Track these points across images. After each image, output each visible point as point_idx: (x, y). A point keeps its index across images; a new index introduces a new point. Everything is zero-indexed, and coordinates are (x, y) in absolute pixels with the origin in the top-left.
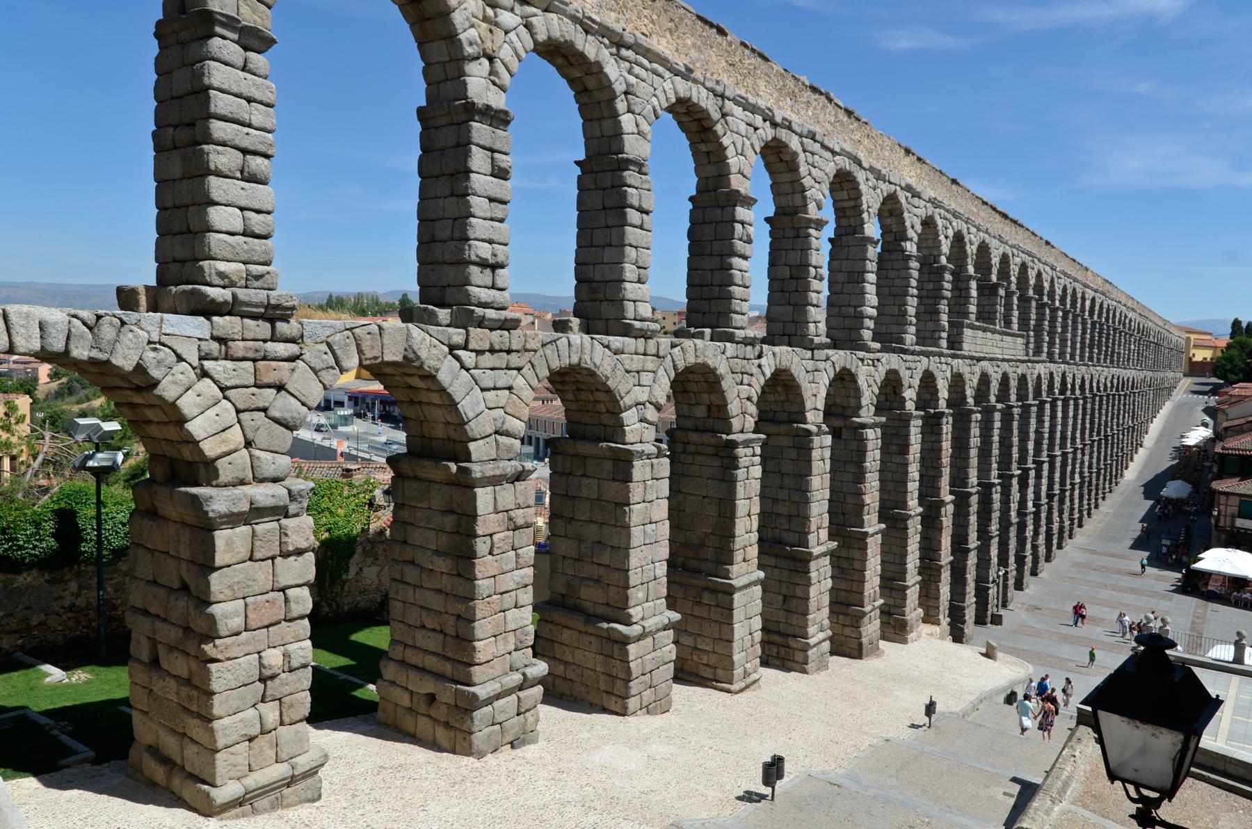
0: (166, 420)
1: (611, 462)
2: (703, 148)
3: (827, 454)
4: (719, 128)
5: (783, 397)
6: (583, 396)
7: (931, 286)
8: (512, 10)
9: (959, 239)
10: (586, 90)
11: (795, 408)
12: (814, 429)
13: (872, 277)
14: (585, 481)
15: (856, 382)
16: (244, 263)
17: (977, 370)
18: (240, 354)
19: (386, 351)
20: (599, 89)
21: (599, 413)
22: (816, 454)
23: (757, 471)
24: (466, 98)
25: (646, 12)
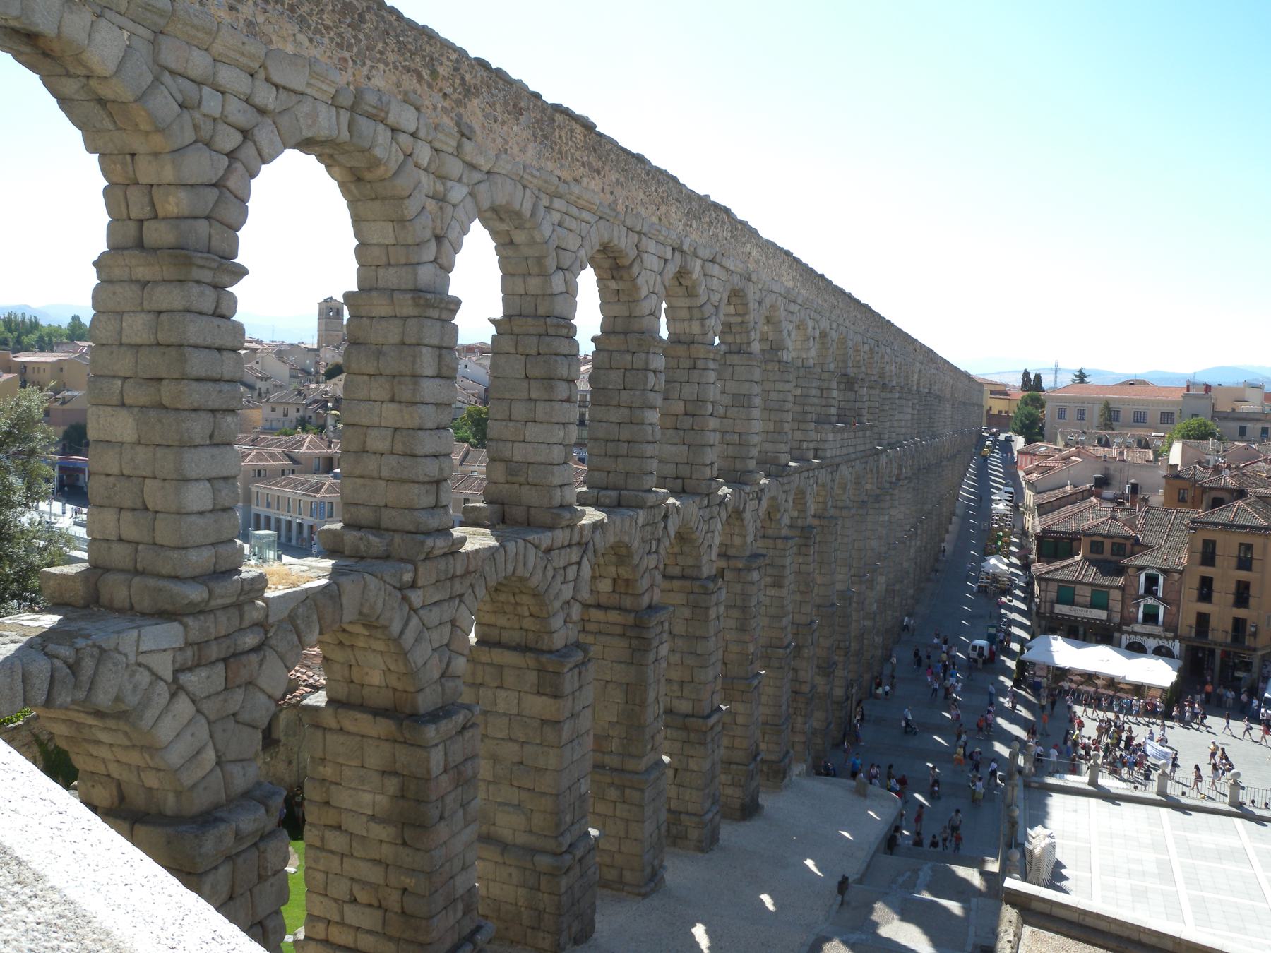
0: (128, 743)
1: (535, 673)
2: (613, 285)
3: (722, 609)
4: (636, 269)
5: (677, 549)
6: (502, 597)
7: (798, 392)
8: (460, 180)
9: (824, 335)
10: (512, 243)
11: (690, 562)
13: (757, 401)
14: (501, 694)
15: (742, 520)
18: (214, 658)
19: (345, 612)
21: (521, 617)
22: (712, 613)
23: (664, 650)
25: (578, 154)
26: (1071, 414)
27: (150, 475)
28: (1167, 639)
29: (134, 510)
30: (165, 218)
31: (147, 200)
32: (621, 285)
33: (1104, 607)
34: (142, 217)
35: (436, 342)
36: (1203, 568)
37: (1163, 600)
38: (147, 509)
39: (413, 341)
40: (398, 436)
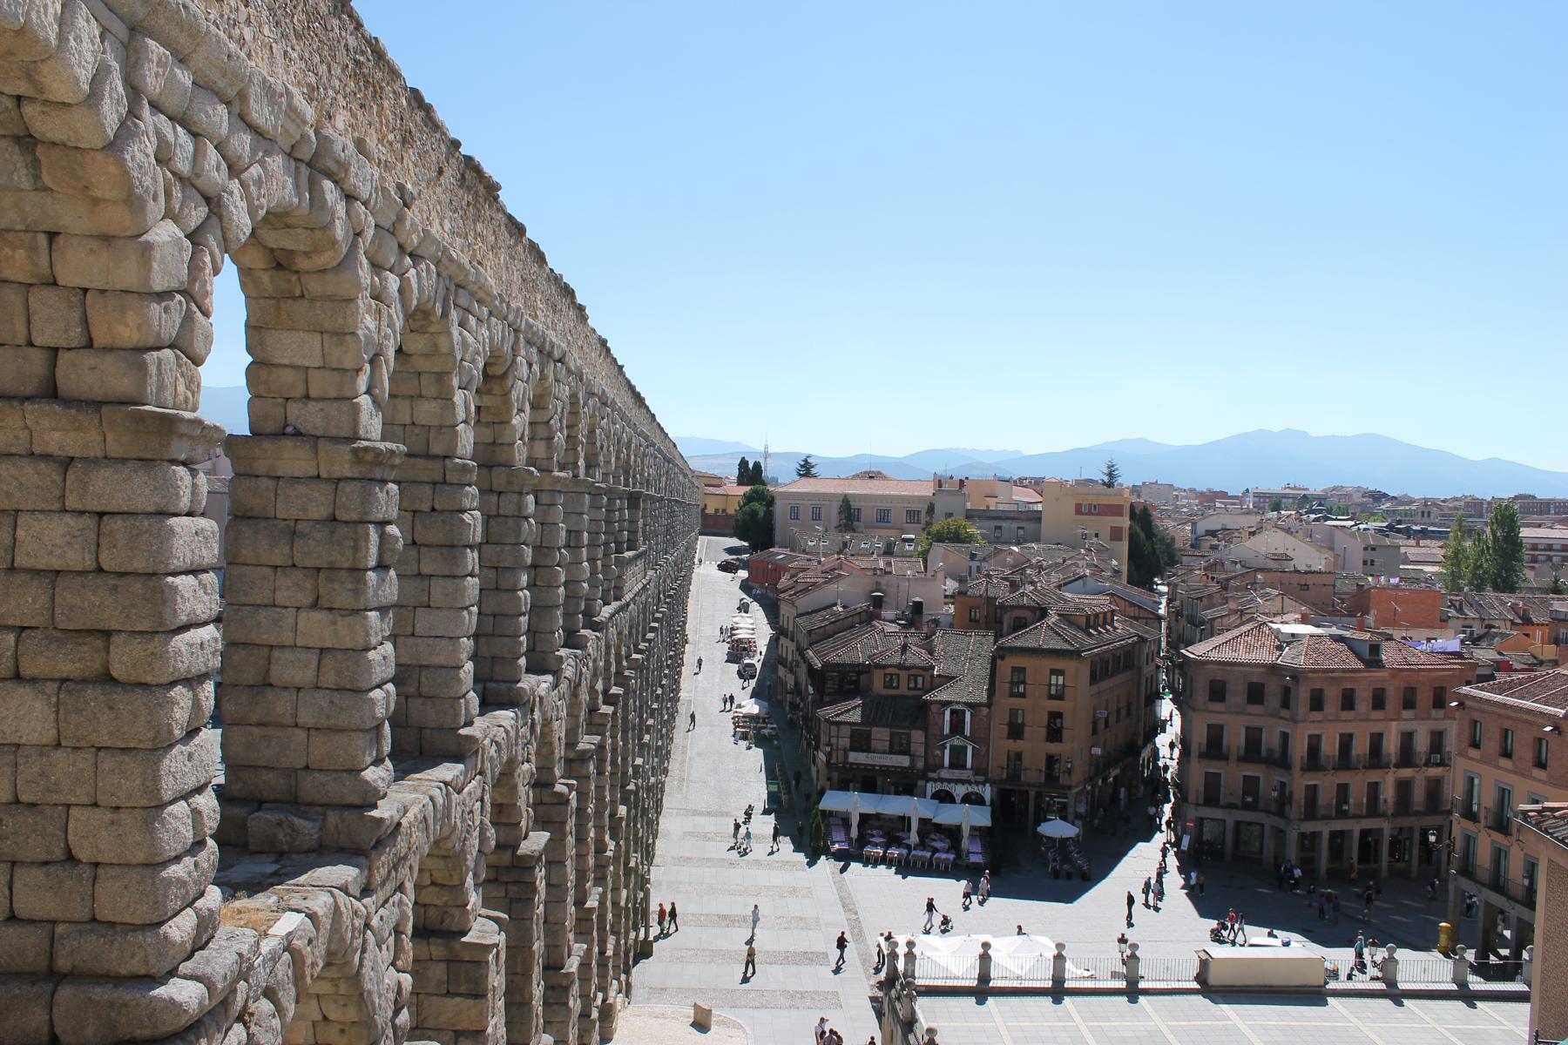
1: (443, 966)
8: (391, 270)
12: (565, 789)
16: (190, 905)
17: (627, 616)
20: (427, 356)
24: (356, 438)
26: (806, 514)
27: (86, 801)
28: (977, 783)
29: (46, 863)
30: (108, 349)
31: (76, 315)
32: (487, 401)
33: (906, 751)
34: (62, 343)
35: (380, 517)
36: (1013, 700)
37: (972, 739)
38: (71, 858)
39: (355, 517)
40: (328, 661)
